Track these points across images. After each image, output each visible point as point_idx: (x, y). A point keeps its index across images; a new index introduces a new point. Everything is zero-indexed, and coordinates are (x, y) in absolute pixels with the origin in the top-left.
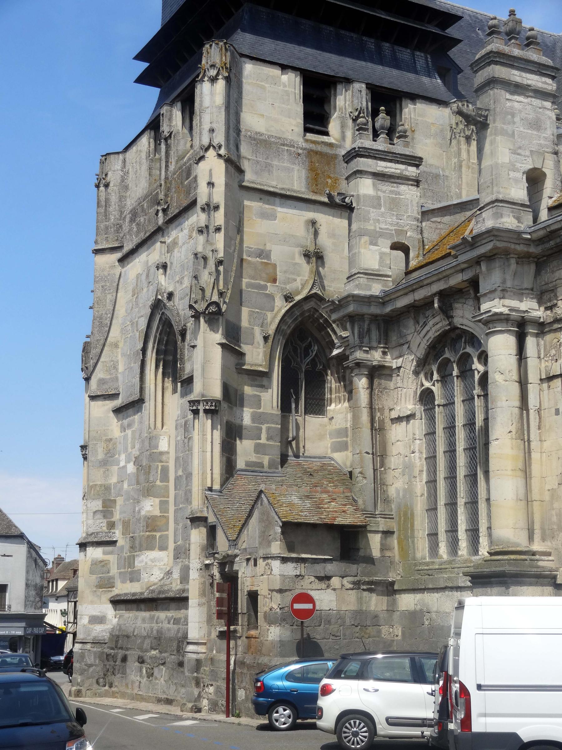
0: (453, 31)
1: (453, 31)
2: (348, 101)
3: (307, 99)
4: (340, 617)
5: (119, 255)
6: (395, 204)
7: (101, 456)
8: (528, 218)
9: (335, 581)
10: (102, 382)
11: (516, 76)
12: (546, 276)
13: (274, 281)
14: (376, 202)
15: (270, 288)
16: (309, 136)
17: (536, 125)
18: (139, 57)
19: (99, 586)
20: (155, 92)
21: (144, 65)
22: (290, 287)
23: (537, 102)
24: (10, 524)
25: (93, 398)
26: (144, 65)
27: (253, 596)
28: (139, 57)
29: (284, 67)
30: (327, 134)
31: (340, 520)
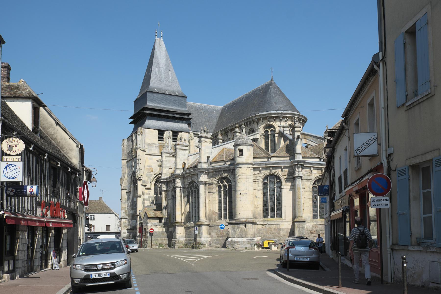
0: (190, 117)
1: (190, 117)
2: (168, 135)
3: (159, 134)
4: (159, 232)
5: (126, 161)
6: (169, 161)
7: (124, 201)
8: (182, 171)
9: (158, 226)
10: (124, 187)
11: (181, 147)
12: (184, 180)
13: (152, 171)
14: (166, 161)
15: (152, 173)
16: (160, 142)
17: (184, 155)
18: (131, 118)
19: (125, 227)
20: (133, 126)
21: (132, 120)
22: (156, 172)
23: (185, 151)
24: (110, 210)
25: (122, 190)
26: (132, 120)
27: (145, 229)
28: (131, 118)
29: (154, 129)
30: (163, 141)
31: (159, 216)
